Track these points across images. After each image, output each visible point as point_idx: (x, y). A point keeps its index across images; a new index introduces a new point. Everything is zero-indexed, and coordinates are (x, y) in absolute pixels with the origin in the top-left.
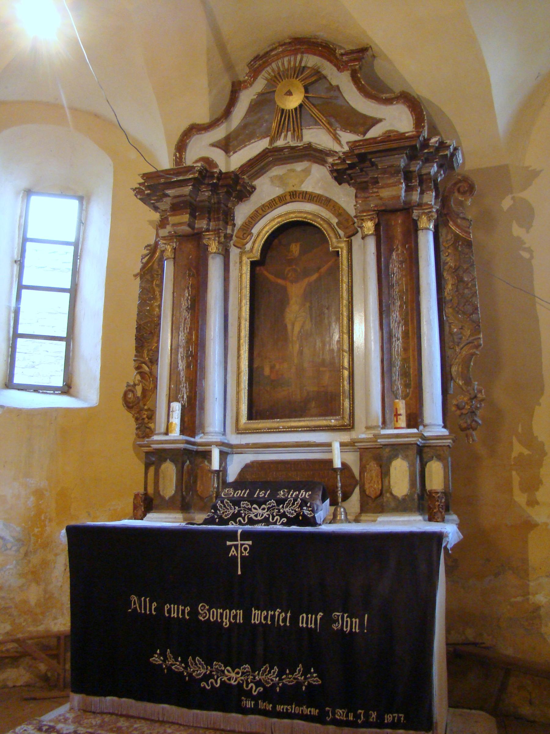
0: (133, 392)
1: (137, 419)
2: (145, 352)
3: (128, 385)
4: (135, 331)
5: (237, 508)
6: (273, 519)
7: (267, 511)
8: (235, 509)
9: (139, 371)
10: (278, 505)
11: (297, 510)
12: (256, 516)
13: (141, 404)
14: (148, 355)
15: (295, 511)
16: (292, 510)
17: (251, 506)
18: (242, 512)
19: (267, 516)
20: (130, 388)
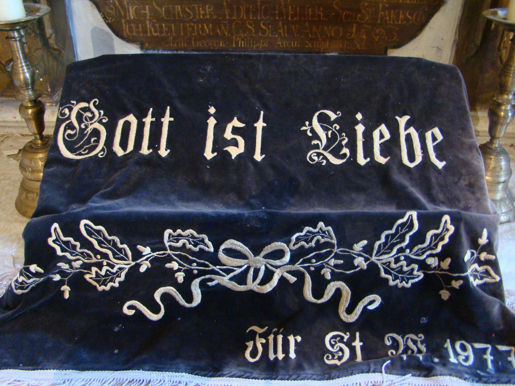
5: (147, 250)
6: (318, 292)
7: (292, 261)
8: (137, 255)
10: (346, 242)
11: (433, 262)
12: (241, 279)
15: (423, 266)
16: (410, 261)
17: (217, 248)
18: (175, 265)
19: (292, 279)
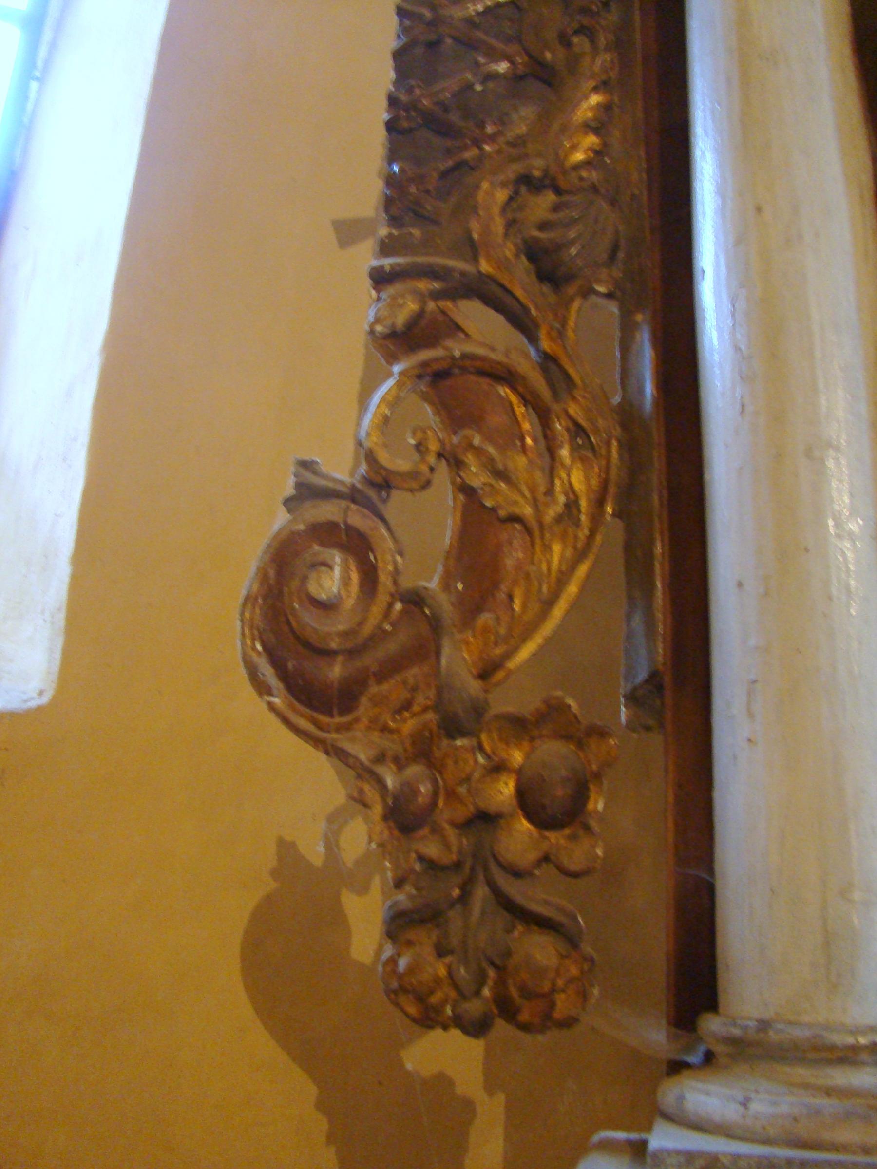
0: (358, 546)
1: (404, 818)
2: (493, 195)
3: (308, 491)
4: (386, 75)
9: (425, 355)
13: (457, 658)
14: (510, 224)
20: (328, 511)
